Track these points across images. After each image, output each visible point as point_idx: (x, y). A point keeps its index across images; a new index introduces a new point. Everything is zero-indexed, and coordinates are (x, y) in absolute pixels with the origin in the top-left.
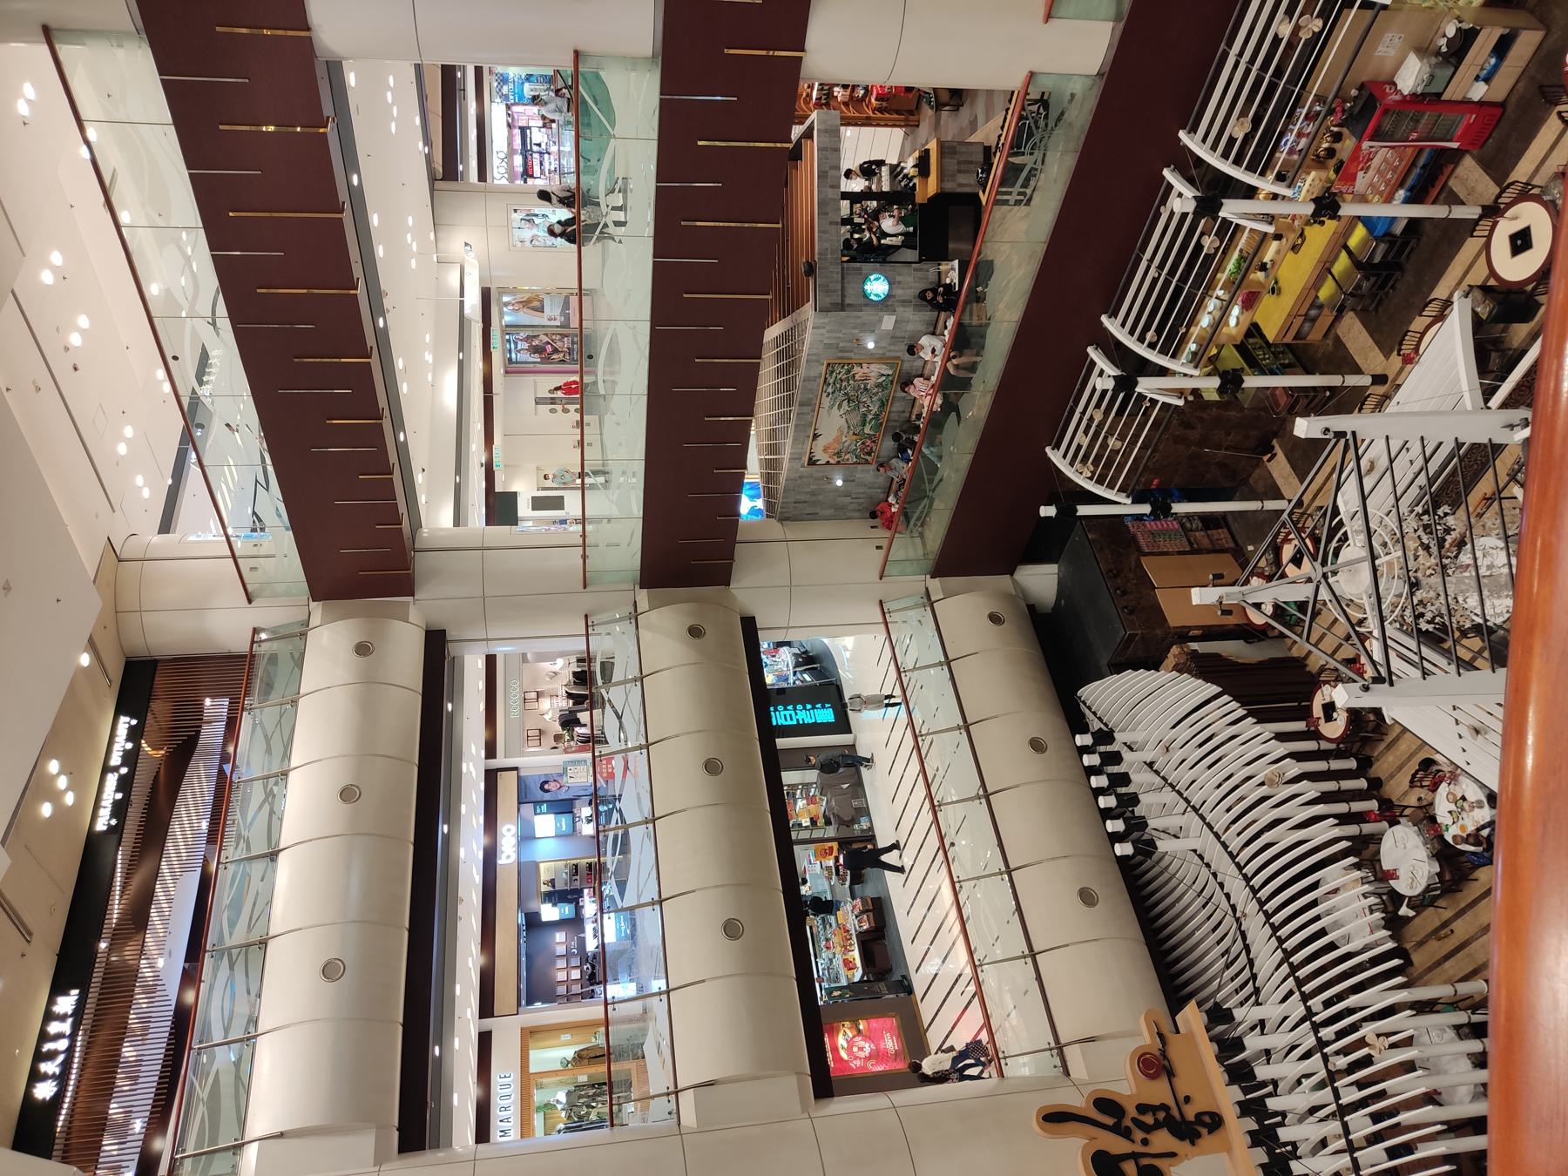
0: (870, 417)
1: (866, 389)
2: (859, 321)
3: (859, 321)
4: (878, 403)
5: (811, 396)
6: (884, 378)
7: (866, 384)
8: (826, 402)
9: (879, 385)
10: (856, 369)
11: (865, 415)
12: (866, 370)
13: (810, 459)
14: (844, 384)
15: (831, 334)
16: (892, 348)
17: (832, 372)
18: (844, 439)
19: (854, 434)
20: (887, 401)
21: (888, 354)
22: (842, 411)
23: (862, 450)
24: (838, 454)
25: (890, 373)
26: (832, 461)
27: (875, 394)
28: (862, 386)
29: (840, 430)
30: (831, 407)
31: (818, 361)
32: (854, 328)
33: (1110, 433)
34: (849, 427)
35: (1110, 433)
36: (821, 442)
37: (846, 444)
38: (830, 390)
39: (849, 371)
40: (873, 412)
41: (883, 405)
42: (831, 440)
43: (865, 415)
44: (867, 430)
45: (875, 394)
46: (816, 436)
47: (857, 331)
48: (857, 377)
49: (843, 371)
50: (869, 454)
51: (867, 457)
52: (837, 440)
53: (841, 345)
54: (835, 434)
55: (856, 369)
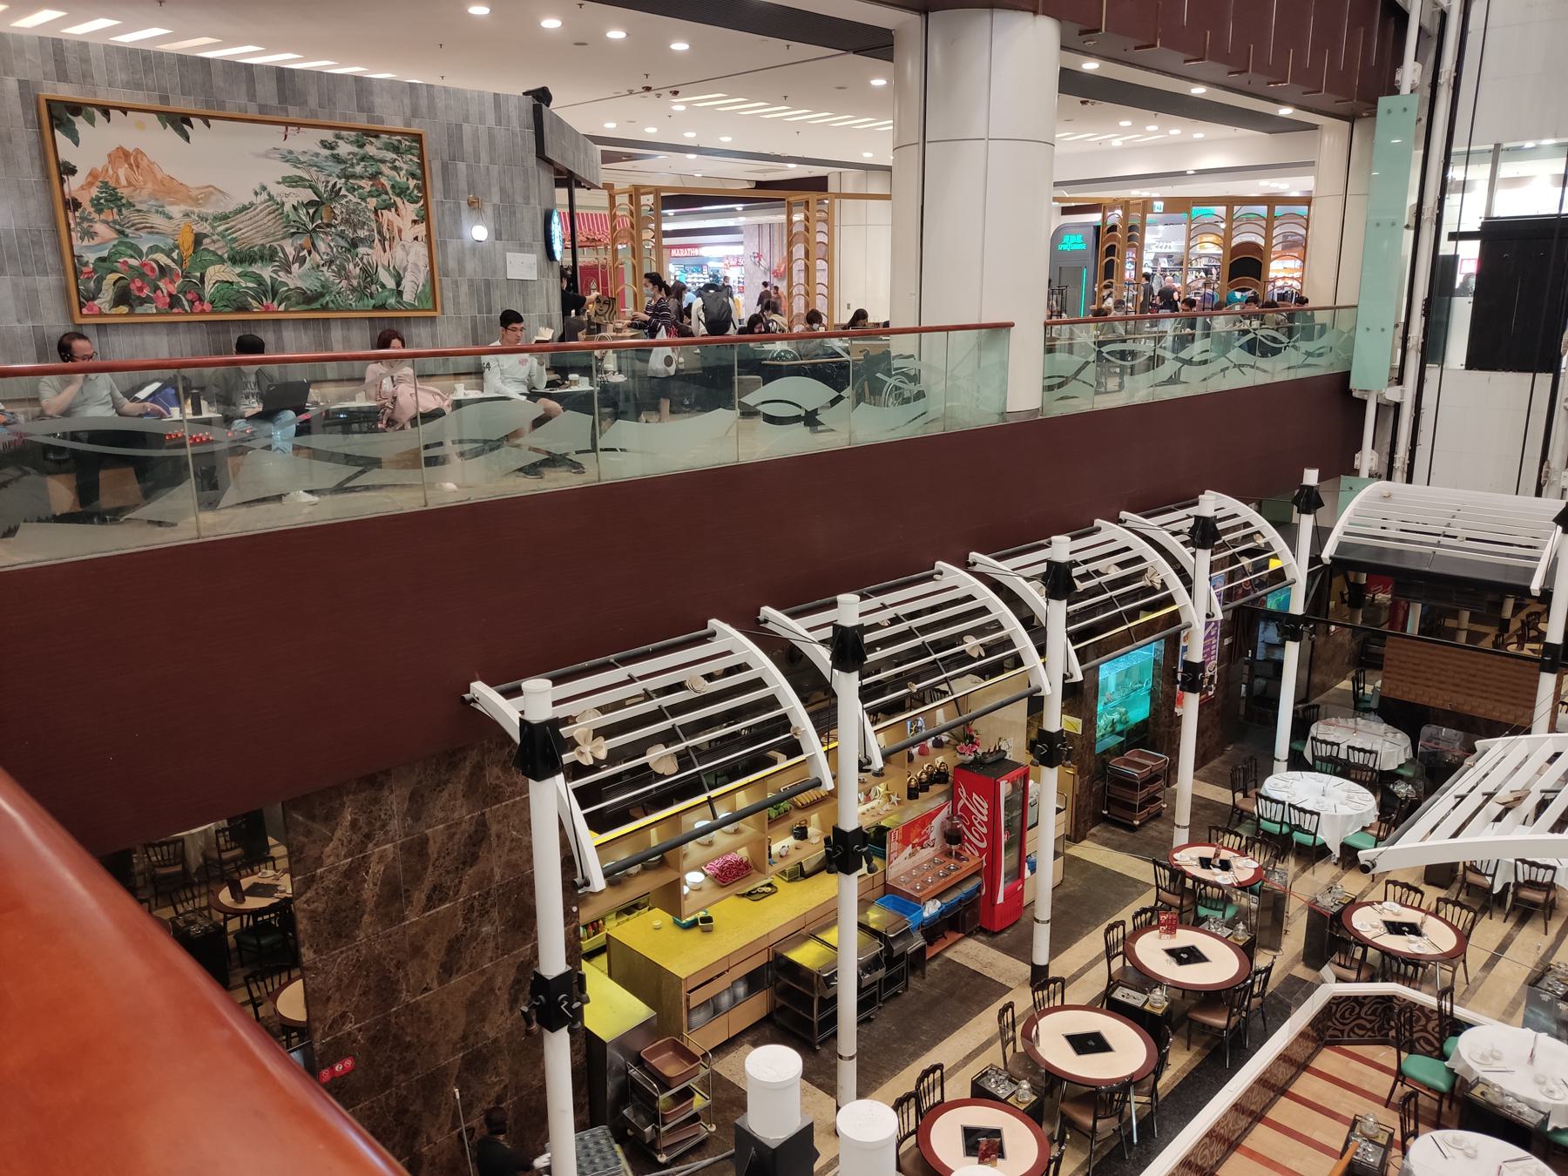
0: (267, 272)
1: (354, 244)
2: (519, 199)
3: (519, 199)
4: (310, 284)
5: (313, 101)
6: (391, 284)
7: (369, 242)
8: (307, 142)
9: (369, 275)
10: (410, 210)
11: (268, 255)
12: (408, 234)
13: (76, 109)
14: (366, 185)
15: (484, 138)
16: (464, 289)
17: (396, 149)
18: (176, 211)
19: (198, 239)
20: (324, 308)
21: (447, 282)
22: (277, 190)
23: (140, 273)
24: (111, 199)
25: (408, 297)
26: (74, 184)
27: (342, 273)
28: (362, 233)
29: (210, 191)
30: (289, 158)
31: (415, 112)
32: (502, 190)
33: (668, 738)
34: (224, 218)
35: (668, 738)
36: (156, 141)
37: (156, 220)
38: (344, 149)
39: (402, 192)
40: (283, 277)
41: (308, 298)
42: (168, 169)
43: (268, 255)
44: (216, 273)
45: (342, 273)
46: (179, 122)
47: (496, 199)
48: (388, 215)
49: (401, 178)
50: (123, 297)
51: (104, 301)
52: (170, 189)
53: (462, 166)
54: (192, 178)
55: (410, 210)
